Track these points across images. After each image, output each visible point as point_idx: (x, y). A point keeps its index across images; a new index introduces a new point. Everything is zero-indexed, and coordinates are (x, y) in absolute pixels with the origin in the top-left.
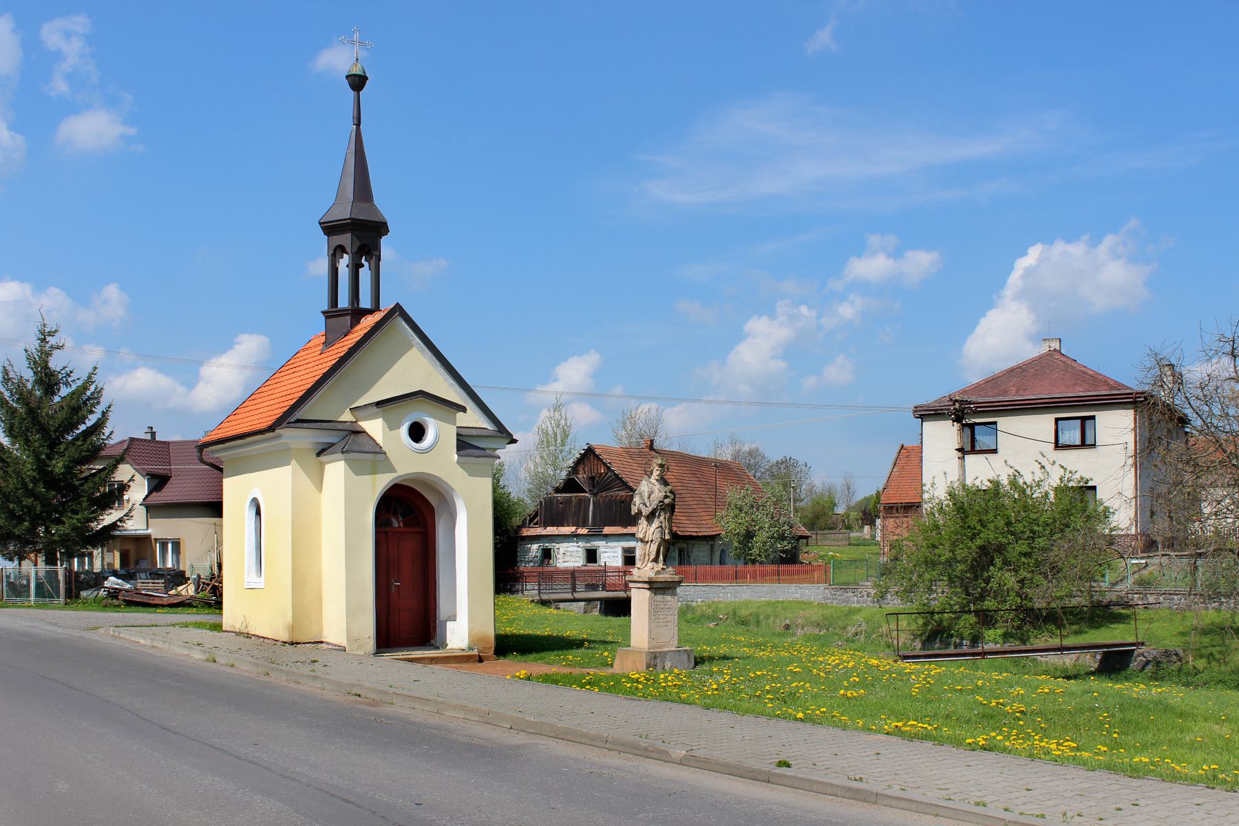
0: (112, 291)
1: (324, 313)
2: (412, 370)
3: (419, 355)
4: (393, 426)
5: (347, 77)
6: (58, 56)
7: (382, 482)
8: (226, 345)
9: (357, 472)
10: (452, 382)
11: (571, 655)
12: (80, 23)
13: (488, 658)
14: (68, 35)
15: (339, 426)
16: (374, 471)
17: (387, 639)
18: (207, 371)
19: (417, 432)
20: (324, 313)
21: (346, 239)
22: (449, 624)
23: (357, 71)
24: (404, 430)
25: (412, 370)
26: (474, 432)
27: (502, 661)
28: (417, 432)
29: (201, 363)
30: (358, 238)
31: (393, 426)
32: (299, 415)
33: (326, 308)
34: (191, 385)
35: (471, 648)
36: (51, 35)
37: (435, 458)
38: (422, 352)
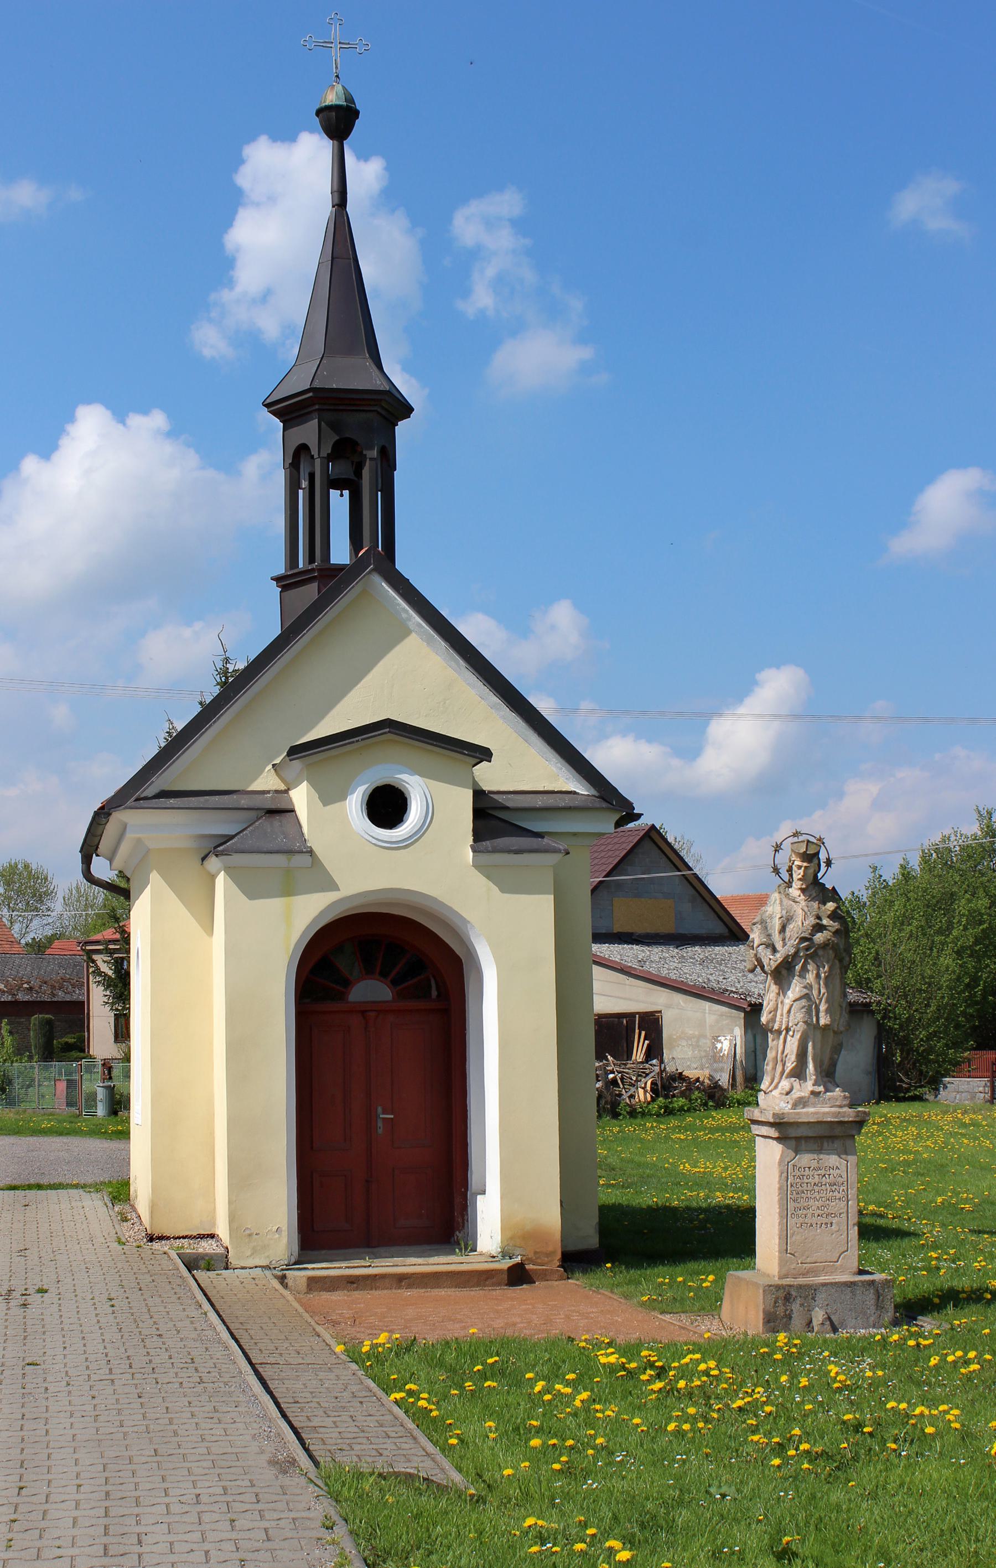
0: (563, 616)
1: (278, 579)
2: (408, 679)
3: (424, 649)
4: (330, 795)
5: (319, 112)
6: (475, 254)
7: (306, 912)
8: (742, 688)
9: (252, 894)
10: (495, 700)
11: (895, 1243)
12: (508, 203)
13: (545, 1275)
14: (490, 224)
15: (244, 802)
16: (288, 889)
17: (322, 1228)
18: (720, 728)
19: (387, 807)
20: (278, 579)
21: (309, 432)
22: (479, 1197)
23: (333, 97)
24: (355, 804)
25: (408, 679)
26: (539, 802)
27: (577, 1282)
28: (387, 807)
29: (716, 713)
30: (334, 426)
31: (330, 795)
32: (165, 780)
33: (281, 570)
34: (692, 752)
35: (505, 1254)
36: (467, 226)
37: (429, 862)
38: (429, 641)
